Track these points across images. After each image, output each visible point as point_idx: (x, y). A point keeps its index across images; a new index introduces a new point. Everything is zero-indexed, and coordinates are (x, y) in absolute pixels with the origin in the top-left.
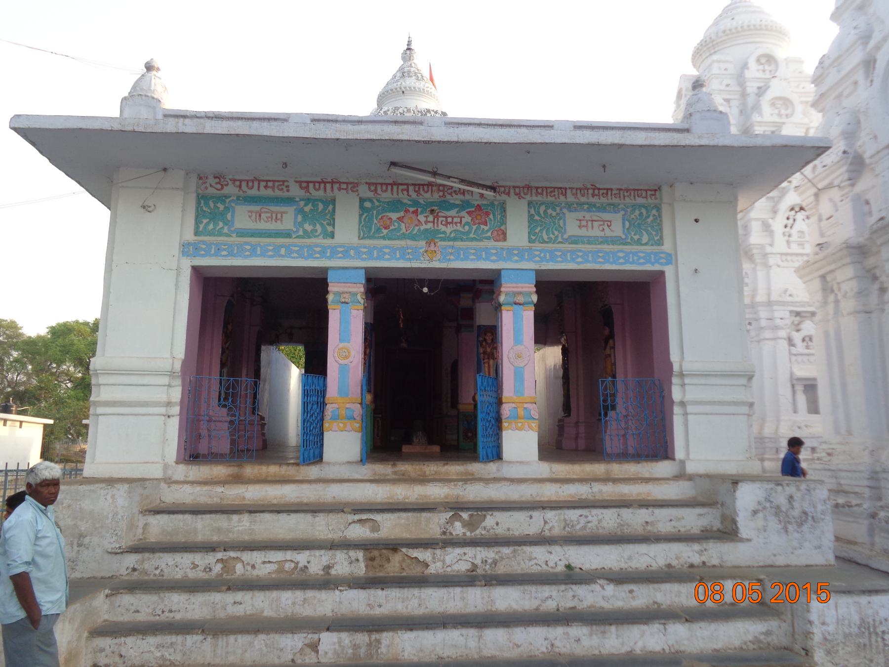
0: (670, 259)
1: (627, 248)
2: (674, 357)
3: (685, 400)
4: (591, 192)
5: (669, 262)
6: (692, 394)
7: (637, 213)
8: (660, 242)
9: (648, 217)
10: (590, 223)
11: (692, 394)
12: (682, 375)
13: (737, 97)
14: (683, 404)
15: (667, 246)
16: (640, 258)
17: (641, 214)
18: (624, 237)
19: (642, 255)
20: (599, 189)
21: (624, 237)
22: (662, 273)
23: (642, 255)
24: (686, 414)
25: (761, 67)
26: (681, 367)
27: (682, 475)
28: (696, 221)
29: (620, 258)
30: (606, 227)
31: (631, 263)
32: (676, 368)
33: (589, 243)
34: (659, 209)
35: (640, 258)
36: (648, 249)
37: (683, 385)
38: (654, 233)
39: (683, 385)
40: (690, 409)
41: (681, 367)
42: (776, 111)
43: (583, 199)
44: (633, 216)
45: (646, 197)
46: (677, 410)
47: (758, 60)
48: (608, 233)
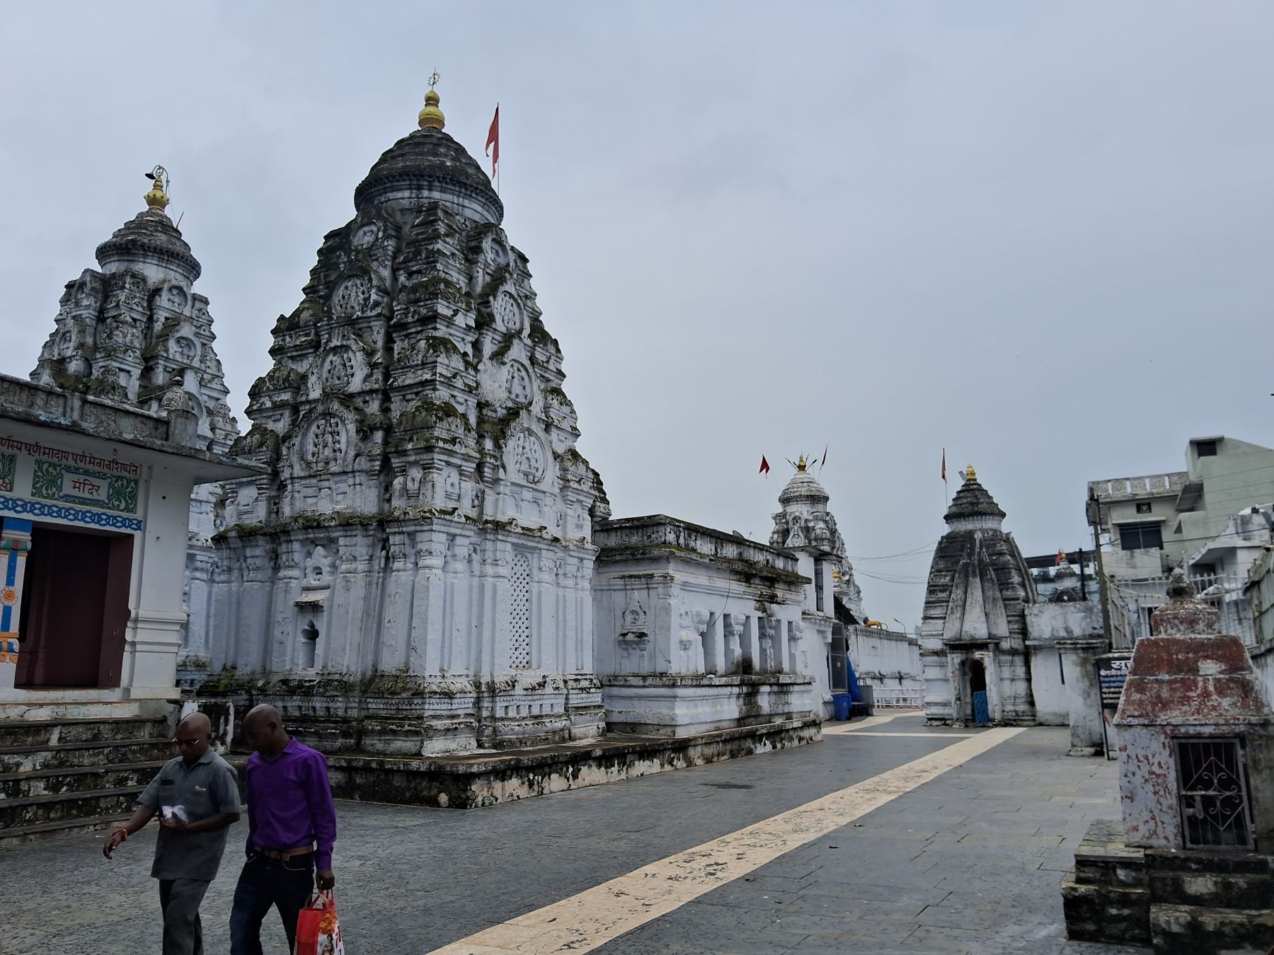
0: (140, 525)
1: (110, 512)
2: (131, 606)
3: (136, 640)
4: (88, 459)
5: (139, 528)
6: (142, 636)
7: (120, 483)
8: (133, 511)
9: (127, 487)
10: (82, 485)
11: (142, 636)
12: (136, 620)
13: (145, 320)
14: (133, 644)
15: (139, 515)
16: (118, 521)
17: (122, 485)
18: (107, 501)
19: (120, 519)
20: (95, 458)
21: (107, 501)
22: (131, 537)
23: (120, 519)
24: (133, 652)
25: (172, 298)
26: (137, 614)
27: (127, 699)
28: (164, 498)
29: (102, 519)
30: (94, 491)
31: (111, 525)
32: (133, 615)
33: (80, 503)
34: (136, 482)
35: (118, 521)
36: (125, 515)
37: (135, 629)
38: (130, 502)
39: (135, 629)
40: (139, 647)
41: (137, 614)
42: (180, 349)
43: (81, 465)
44: (116, 485)
45: (129, 472)
46: (127, 648)
47: (170, 289)
48: (95, 497)
